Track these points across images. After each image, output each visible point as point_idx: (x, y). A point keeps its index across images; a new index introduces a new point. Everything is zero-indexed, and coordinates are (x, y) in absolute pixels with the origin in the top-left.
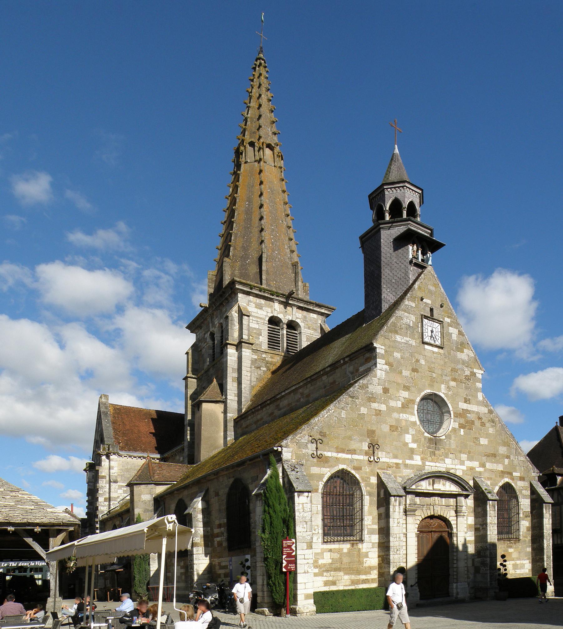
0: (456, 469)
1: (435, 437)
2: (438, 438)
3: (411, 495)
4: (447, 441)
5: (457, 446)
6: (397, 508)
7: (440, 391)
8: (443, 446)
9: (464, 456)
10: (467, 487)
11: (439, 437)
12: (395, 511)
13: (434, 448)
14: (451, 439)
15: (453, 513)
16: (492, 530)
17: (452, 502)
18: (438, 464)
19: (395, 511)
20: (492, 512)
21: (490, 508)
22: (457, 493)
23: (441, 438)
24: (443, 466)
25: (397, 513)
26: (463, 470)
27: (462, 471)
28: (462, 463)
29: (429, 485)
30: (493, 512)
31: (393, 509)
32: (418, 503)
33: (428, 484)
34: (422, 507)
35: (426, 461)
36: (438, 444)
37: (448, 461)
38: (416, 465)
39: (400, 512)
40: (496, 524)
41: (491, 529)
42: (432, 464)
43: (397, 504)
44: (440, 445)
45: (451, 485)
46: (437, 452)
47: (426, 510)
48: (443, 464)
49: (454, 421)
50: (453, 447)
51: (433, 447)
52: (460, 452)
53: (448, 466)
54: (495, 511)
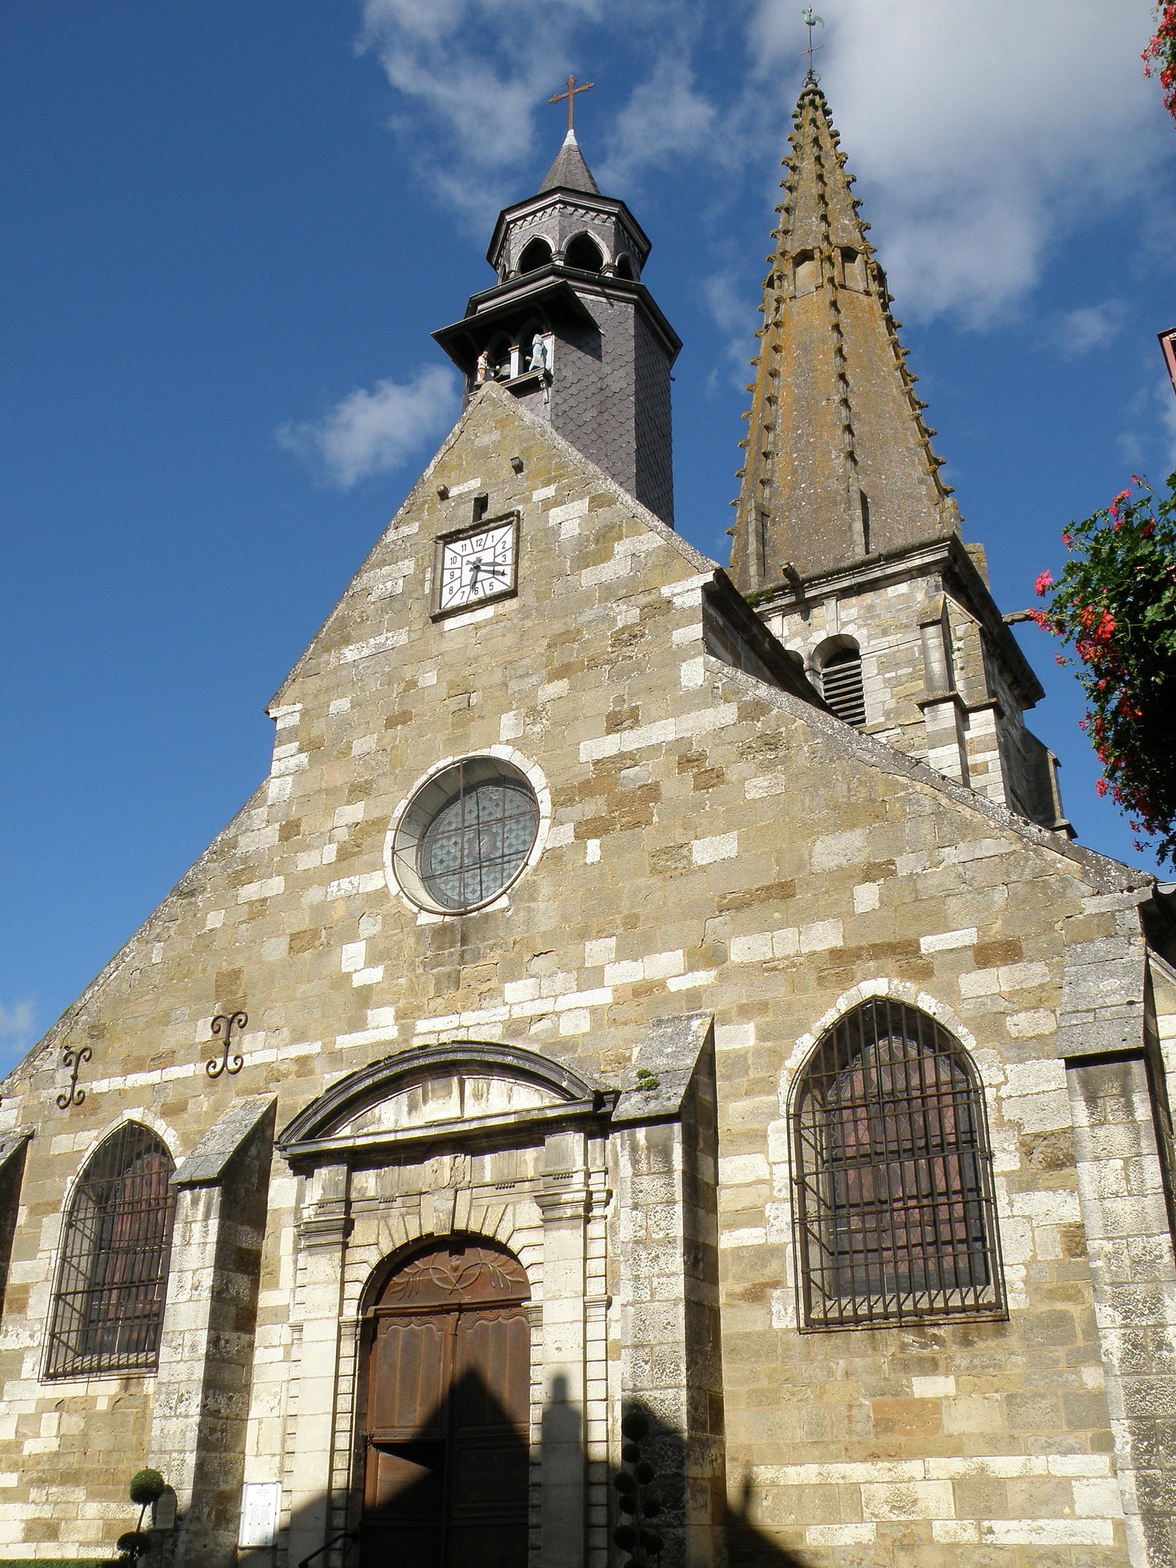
0: (558, 1014)
1: (461, 914)
2: (476, 913)
3: (330, 1168)
4: (516, 912)
5: (564, 918)
6: (197, 1228)
7: (492, 738)
8: (497, 936)
9: (599, 950)
10: (564, 1084)
11: (478, 909)
12: (189, 1244)
13: (456, 957)
14: (534, 899)
15: (530, 1213)
16: (649, 1278)
17: (531, 1165)
18: (468, 1018)
19: (189, 1244)
20: (646, 1183)
21: (635, 1162)
22: (511, 1119)
23: (489, 909)
24: (493, 1019)
25: (194, 1250)
26: (593, 1010)
27: (586, 1013)
28: (591, 978)
29: (410, 1112)
30: (659, 1182)
31: (184, 1237)
32: (371, 1193)
33: (405, 1109)
34: (382, 1206)
35: (419, 1018)
36: (472, 939)
37: (515, 991)
38: (372, 1045)
39: (205, 1244)
40: (680, 1243)
41: (644, 1271)
42: (439, 1023)
43: (200, 1216)
44: (484, 939)
45: (515, 1088)
46: (467, 971)
47: (403, 1216)
48: (491, 1013)
49: (556, 822)
50: (542, 929)
51: (452, 954)
52: (583, 935)
53: (517, 1013)
54: (669, 1172)
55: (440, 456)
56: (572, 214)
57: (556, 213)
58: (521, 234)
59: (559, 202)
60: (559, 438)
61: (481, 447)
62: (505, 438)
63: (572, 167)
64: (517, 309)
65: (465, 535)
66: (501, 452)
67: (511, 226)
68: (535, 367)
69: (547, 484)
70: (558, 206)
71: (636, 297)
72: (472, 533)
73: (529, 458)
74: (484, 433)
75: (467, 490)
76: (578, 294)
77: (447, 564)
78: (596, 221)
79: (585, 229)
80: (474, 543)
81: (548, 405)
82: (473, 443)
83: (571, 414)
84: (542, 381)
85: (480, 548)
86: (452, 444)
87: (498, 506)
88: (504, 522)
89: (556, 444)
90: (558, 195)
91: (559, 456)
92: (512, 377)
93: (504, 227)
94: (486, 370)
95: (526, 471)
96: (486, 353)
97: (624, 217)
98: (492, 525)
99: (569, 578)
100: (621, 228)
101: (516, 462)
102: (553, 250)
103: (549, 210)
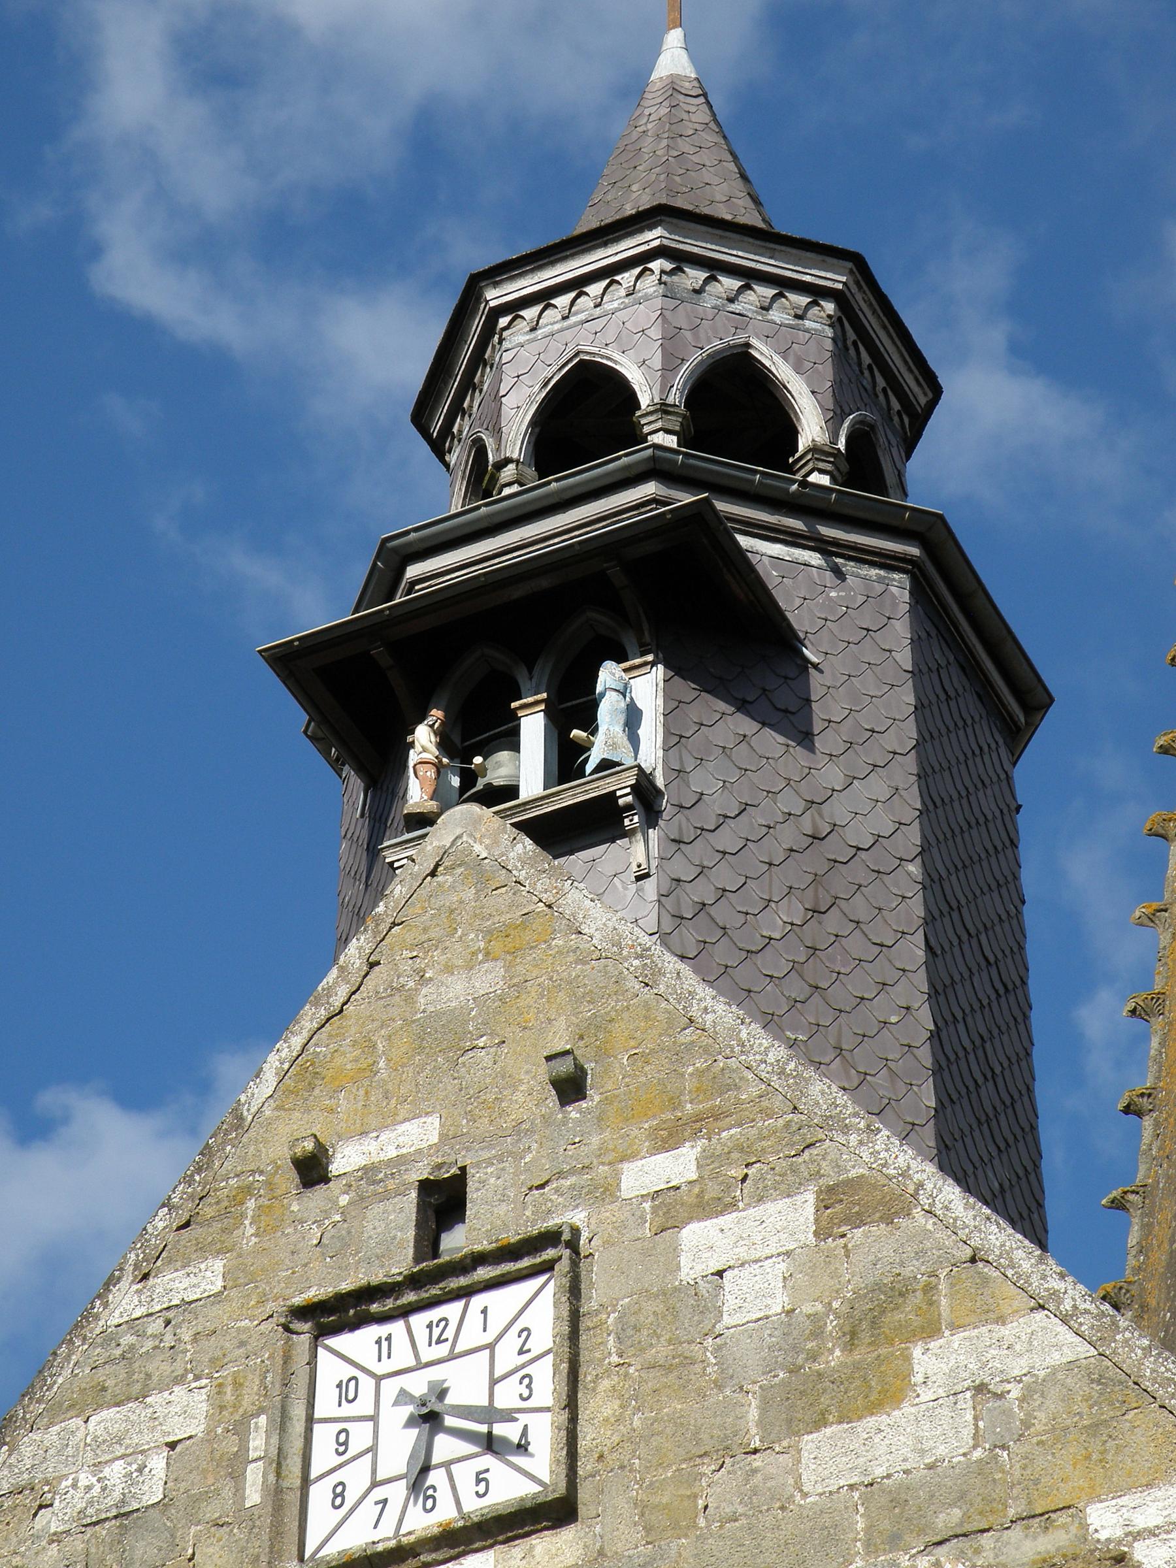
55: (297, 1041)
56: (698, 292)
57: (649, 285)
58: (535, 347)
59: (661, 252)
60: (705, 992)
61: (438, 1015)
62: (520, 987)
63: (684, 146)
64: (544, 583)
65: (390, 1304)
66: (508, 1033)
67: (503, 321)
68: (606, 765)
69: (668, 1140)
70: (656, 265)
71: (914, 551)
72: (410, 1297)
73: (603, 1053)
74: (449, 969)
75: (392, 1153)
76: (744, 541)
77: (326, 1403)
78: (776, 315)
79: (740, 338)
80: (421, 1335)
81: (650, 885)
82: (410, 999)
83: (721, 913)
84: (629, 807)
85: (443, 1350)
86: (337, 1002)
87: (502, 1209)
88: (525, 1263)
89: (695, 1012)
90: (658, 231)
91: (706, 1050)
92: (525, 794)
93: (477, 325)
94: (439, 767)
95: (594, 1097)
96: (436, 714)
97: (861, 301)
98: (483, 1273)
99: (757, 1461)
100: (851, 335)
101: (564, 1067)
102: (644, 400)
103: (627, 278)
